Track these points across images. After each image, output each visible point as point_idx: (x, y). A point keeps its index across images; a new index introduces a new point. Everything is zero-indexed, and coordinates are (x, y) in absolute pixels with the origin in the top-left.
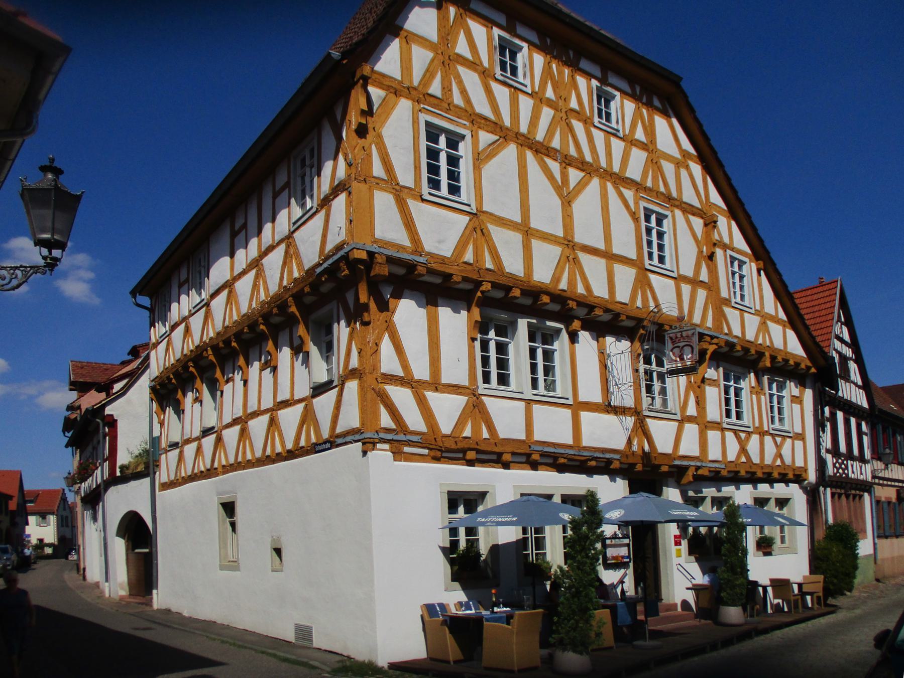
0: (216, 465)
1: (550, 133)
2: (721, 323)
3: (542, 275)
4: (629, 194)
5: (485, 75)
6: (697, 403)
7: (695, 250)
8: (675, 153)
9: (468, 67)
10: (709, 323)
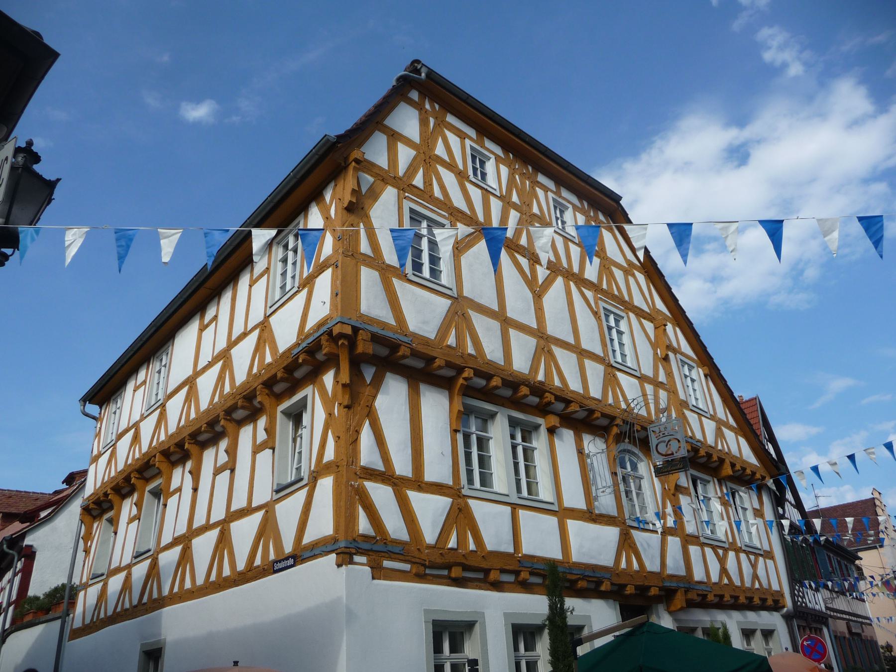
2: (685, 427)
3: (521, 363)
4: (589, 294)
5: (461, 176)
9: (447, 168)
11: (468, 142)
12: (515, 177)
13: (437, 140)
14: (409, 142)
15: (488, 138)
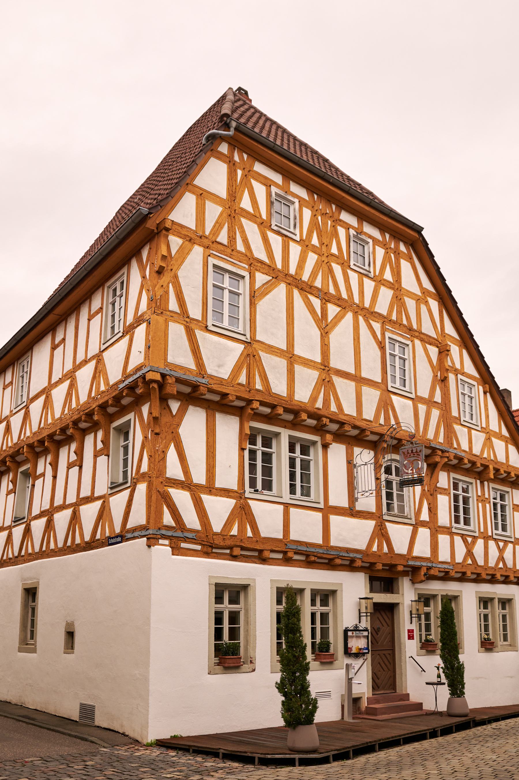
0: (23, 553)
1: (314, 275)
3: (303, 394)
5: (264, 226)
6: (430, 509)
7: (431, 375)
8: (418, 292)
10: (441, 439)
11: (274, 189)
12: (317, 219)
13: (243, 191)
14: (215, 198)
15: (294, 181)
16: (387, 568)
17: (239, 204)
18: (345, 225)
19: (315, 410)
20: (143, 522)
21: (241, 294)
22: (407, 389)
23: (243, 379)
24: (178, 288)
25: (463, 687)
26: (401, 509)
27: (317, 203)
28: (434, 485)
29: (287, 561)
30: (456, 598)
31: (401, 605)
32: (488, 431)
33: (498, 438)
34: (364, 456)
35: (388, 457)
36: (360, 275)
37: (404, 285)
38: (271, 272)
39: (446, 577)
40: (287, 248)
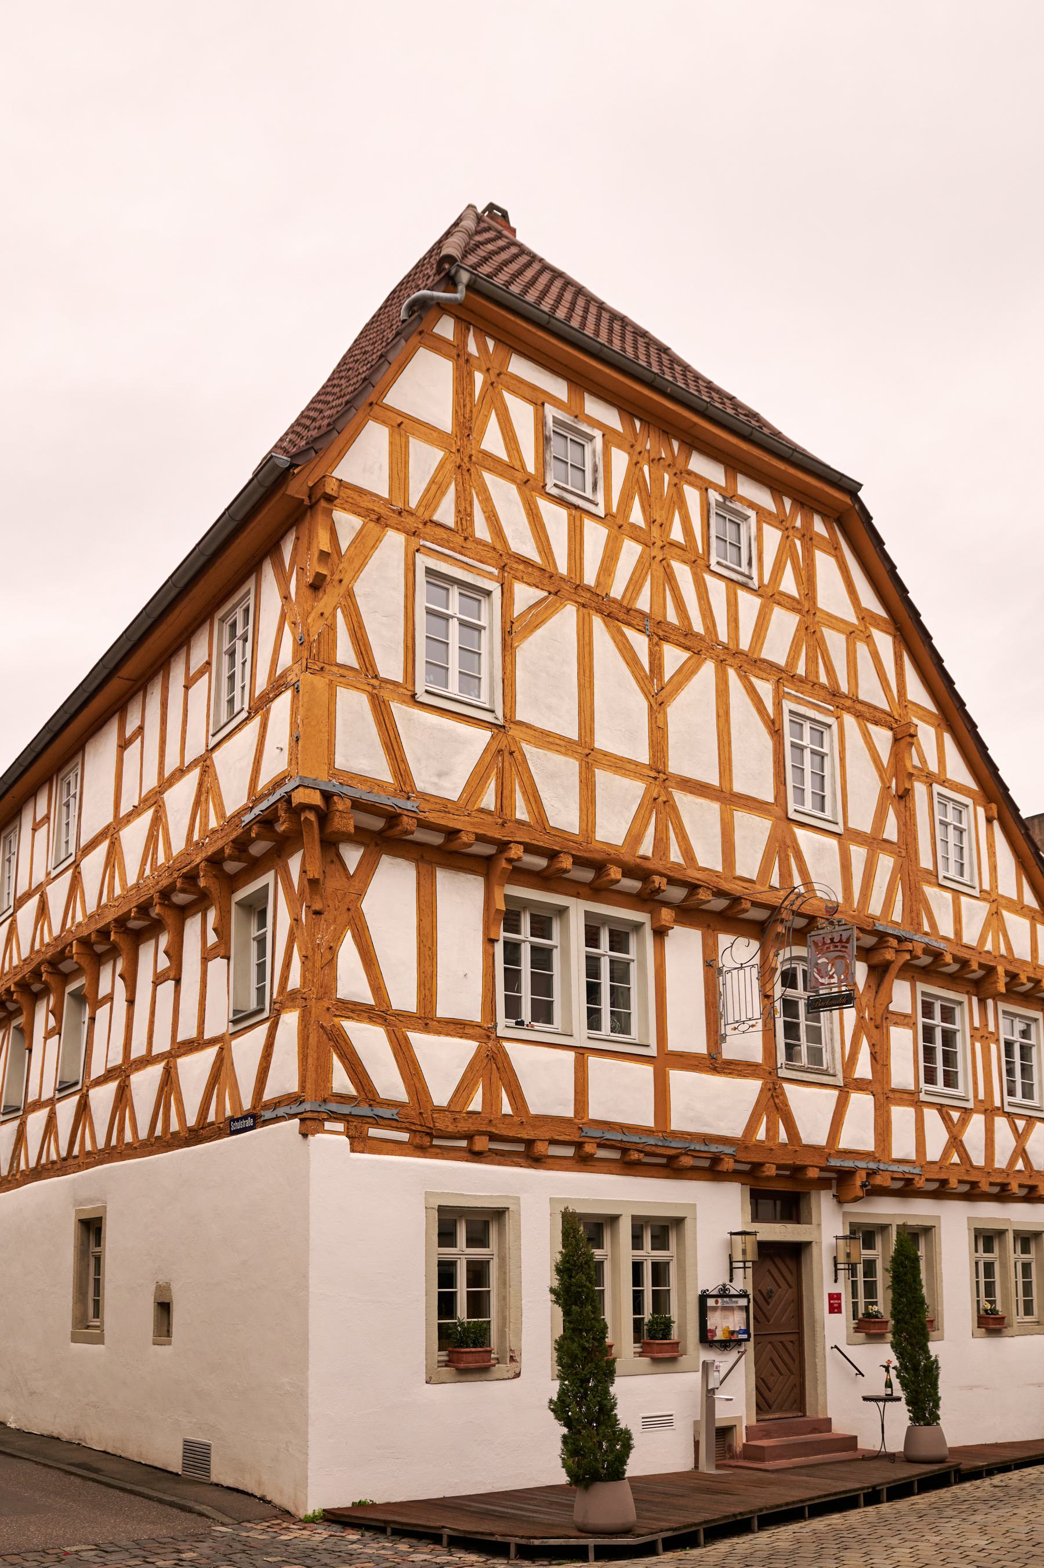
1: (634, 585)
3: (612, 829)
5: (530, 487)
6: (874, 1056)
8: (852, 618)
10: (897, 916)
11: (550, 412)
12: (641, 470)
13: (487, 417)
14: (429, 432)
15: (592, 393)
16: (788, 1173)
17: (479, 442)
18: (699, 482)
19: (638, 860)
20: (294, 1087)
21: (484, 628)
22: (828, 814)
23: (489, 800)
24: (354, 618)
25: (937, 1406)
26: (816, 1055)
27: (640, 438)
28: (884, 1007)
29: (583, 1161)
30: (927, 1230)
31: (815, 1248)
32: (994, 897)
33: (1016, 912)
34: (739, 952)
35: (785, 953)
36: (731, 584)
37: (822, 603)
38: (546, 581)
39: (906, 1189)
40: (578, 532)
